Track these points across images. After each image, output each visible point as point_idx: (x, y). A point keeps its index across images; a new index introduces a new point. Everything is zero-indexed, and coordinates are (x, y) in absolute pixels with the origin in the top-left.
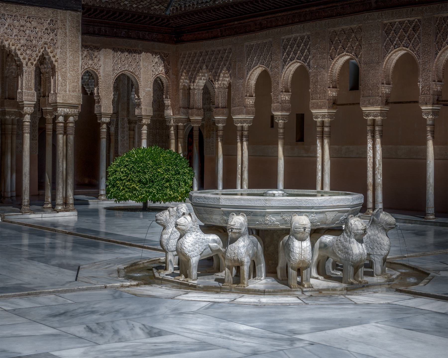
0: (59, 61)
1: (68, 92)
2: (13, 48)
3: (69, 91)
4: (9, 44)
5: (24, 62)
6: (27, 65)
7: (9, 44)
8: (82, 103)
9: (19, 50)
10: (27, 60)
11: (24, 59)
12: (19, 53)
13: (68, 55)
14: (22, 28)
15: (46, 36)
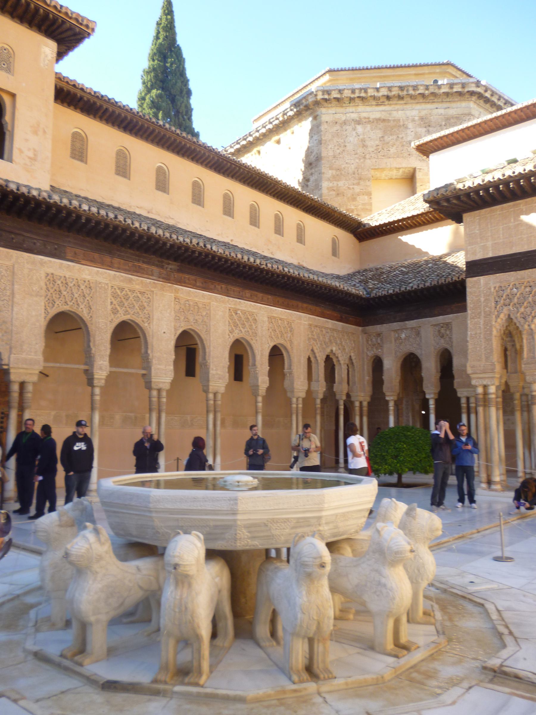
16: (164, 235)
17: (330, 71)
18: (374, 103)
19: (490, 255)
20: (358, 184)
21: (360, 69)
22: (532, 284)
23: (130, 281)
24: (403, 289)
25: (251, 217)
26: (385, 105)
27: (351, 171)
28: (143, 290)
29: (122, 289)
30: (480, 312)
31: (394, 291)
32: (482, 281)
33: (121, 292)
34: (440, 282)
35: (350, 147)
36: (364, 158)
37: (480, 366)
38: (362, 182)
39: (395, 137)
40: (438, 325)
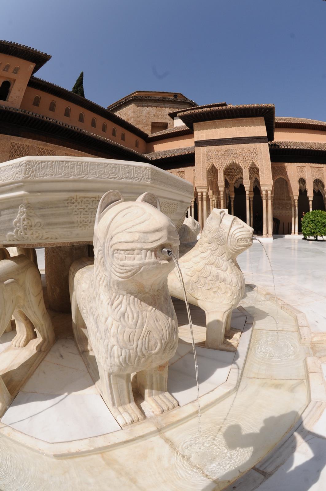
0: (259, 165)
1: (265, 179)
2: (237, 162)
3: (266, 179)
4: (235, 161)
5: (243, 168)
6: (244, 168)
7: (235, 161)
8: (273, 184)
9: (240, 163)
10: (244, 167)
11: (243, 166)
12: (240, 164)
13: (264, 163)
14: (241, 154)
15: (252, 155)
16: (63, 125)
17: (138, 92)
18: (153, 101)
19: (205, 139)
20: (146, 127)
21: (149, 92)
22: (221, 151)
23: (46, 145)
24: (165, 157)
25: (103, 129)
26: (157, 102)
27: (144, 122)
28: (51, 149)
29: (42, 149)
30: (201, 161)
31: (161, 157)
32: (201, 149)
33: (42, 150)
34: (181, 154)
35: (143, 114)
36: (149, 118)
37: (200, 183)
38: (147, 126)
39: (161, 112)
40: (180, 172)
